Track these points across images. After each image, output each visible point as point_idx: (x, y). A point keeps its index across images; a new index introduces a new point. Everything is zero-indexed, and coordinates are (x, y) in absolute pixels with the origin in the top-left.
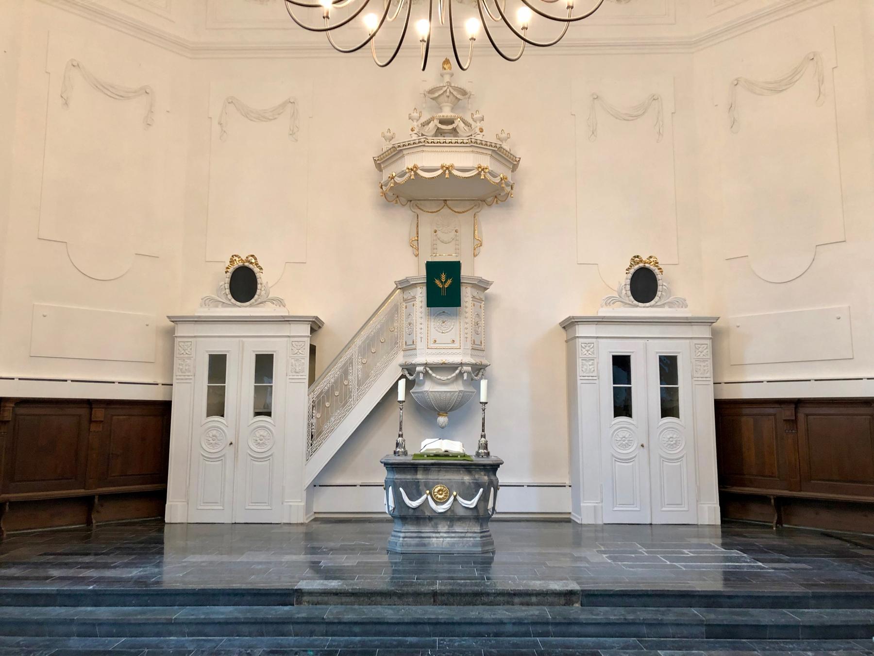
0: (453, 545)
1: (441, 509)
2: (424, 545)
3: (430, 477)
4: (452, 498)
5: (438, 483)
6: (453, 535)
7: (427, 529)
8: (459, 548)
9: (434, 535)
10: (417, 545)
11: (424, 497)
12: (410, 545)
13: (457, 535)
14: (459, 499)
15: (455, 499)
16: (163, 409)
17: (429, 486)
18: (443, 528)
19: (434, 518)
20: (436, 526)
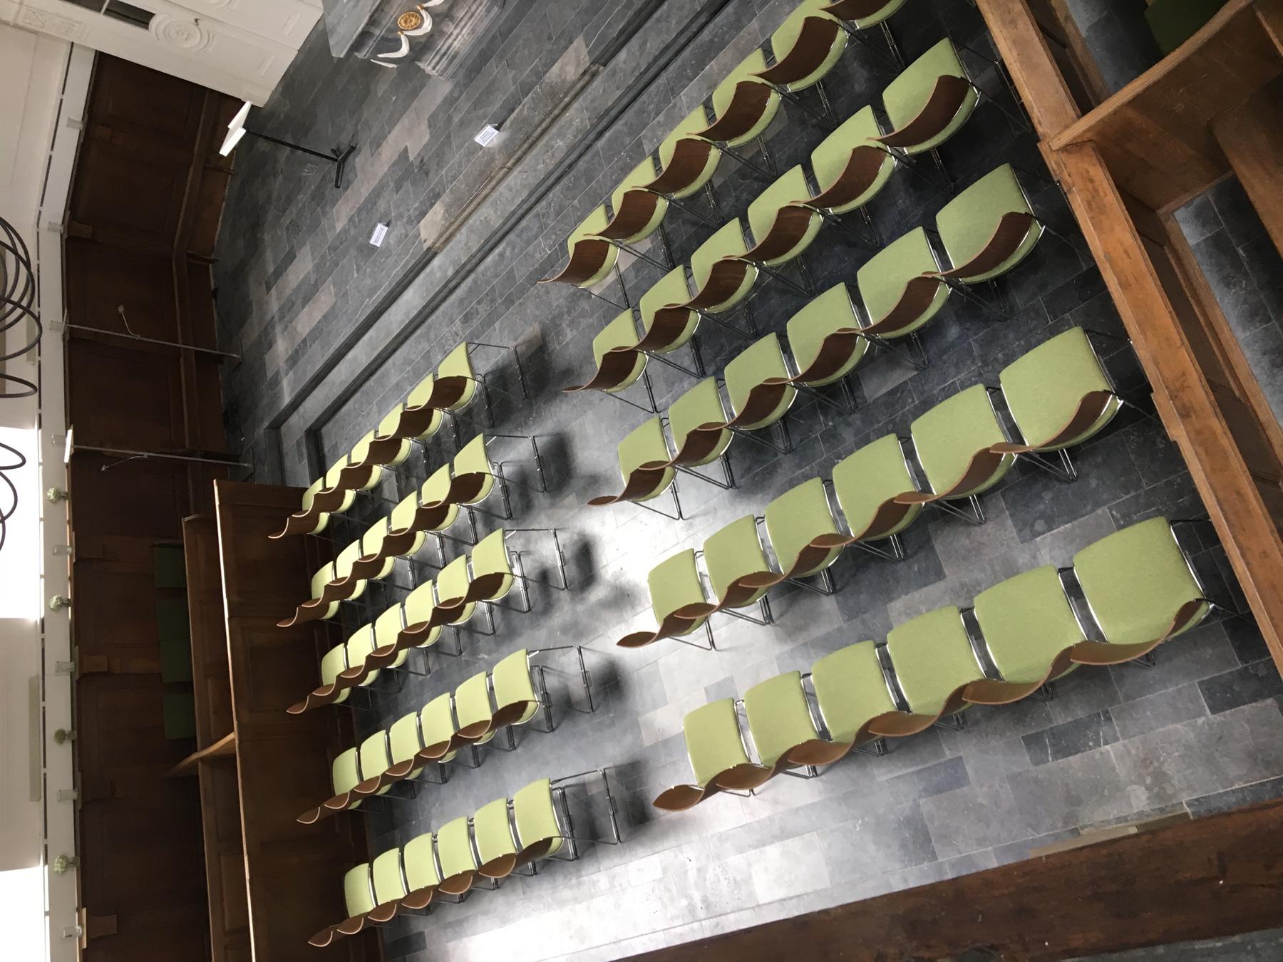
0: (473, 31)
1: (427, 25)
2: (454, 57)
3: (384, 23)
4: (424, 13)
5: (396, 19)
6: (462, 24)
7: (442, 45)
8: (481, 29)
9: (450, 41)
10: (450, 63)
11: (403, 38)
12: (446, 69)
13: (466, 19)
14: (425, 5)
15: (426, 9)
16: (103, 62)
17: (395, 29)
18: (449, 28)
19: (431, 36)
20: (442, 33)
